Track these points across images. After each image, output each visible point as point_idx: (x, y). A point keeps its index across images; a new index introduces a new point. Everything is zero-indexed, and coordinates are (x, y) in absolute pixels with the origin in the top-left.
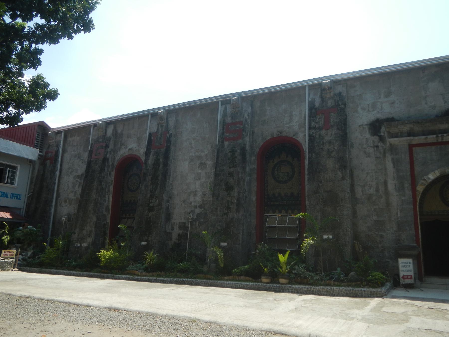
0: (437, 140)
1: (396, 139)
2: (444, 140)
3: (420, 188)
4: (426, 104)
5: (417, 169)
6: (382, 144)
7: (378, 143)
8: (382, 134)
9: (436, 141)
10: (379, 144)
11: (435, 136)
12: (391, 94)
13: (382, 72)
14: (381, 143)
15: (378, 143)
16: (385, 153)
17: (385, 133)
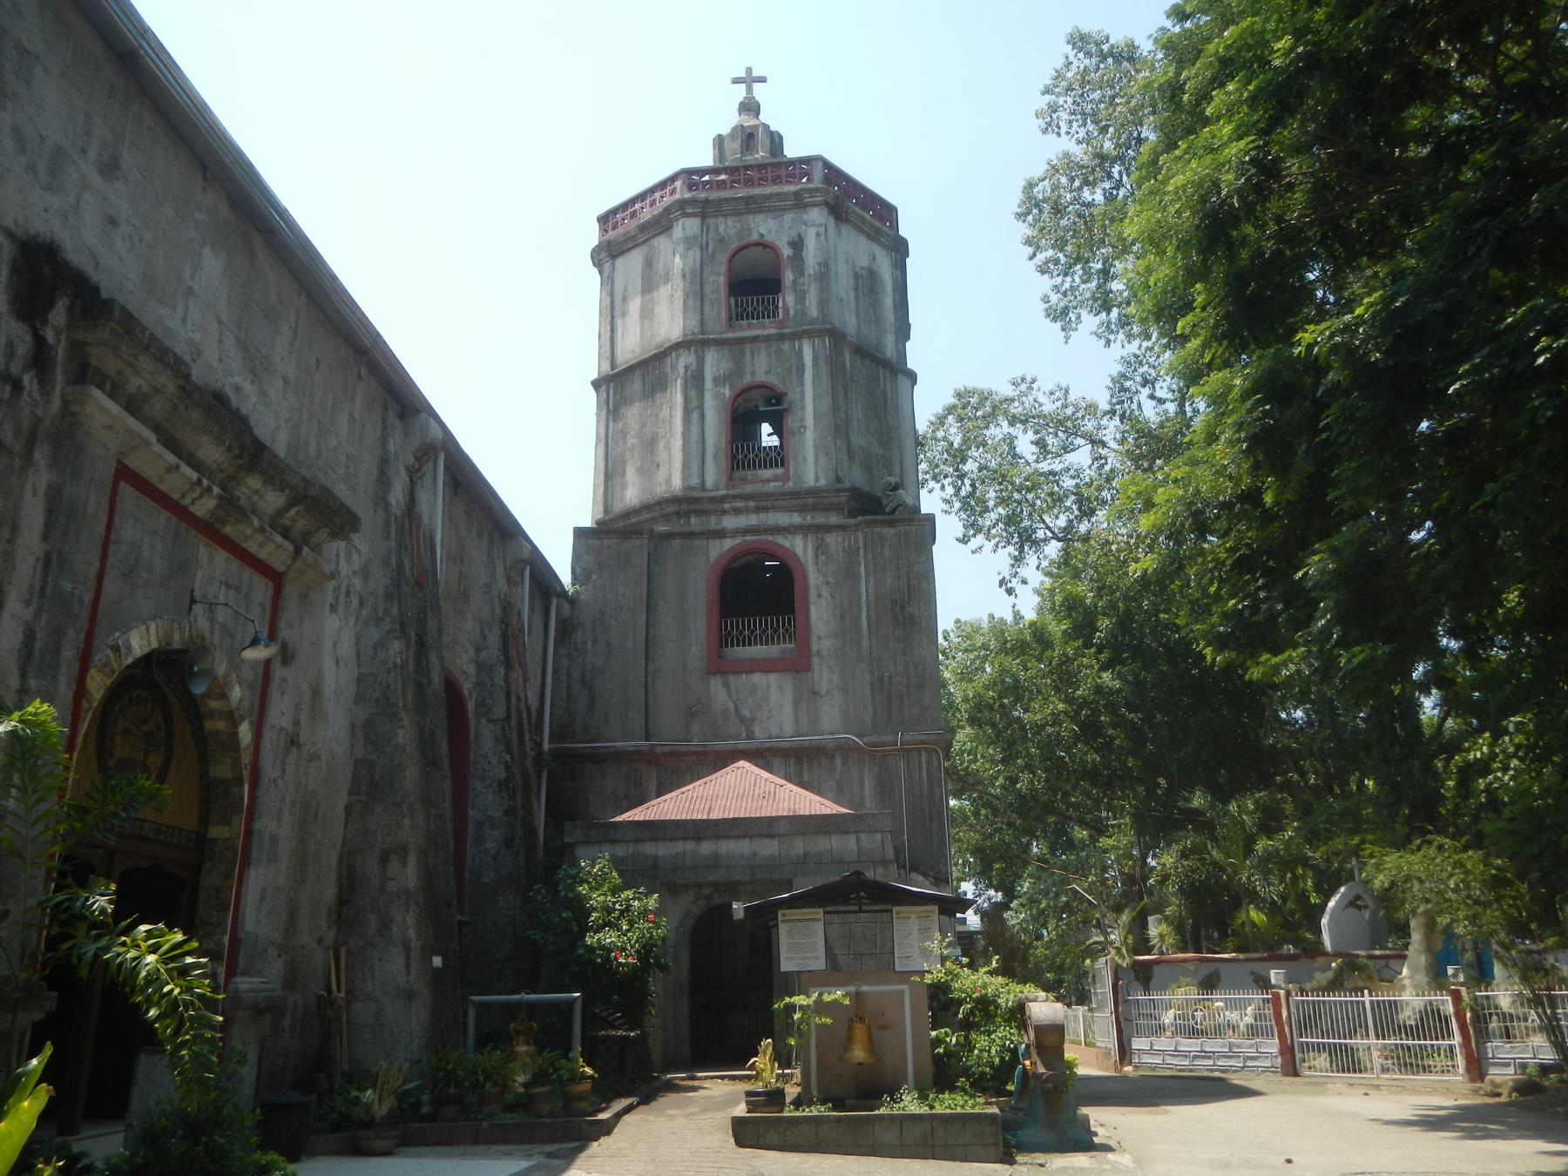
0: (183, 496)
1: (113, 407)
2: (192, 509)
3: (98, 684)
4: (184, 320)
5: (111, 588)
6: (35, 387)
7: (24, 370)
8: (50, 335)
9: (176, 496)
10: (26, 379)
11: (195, 476)
12: (118, 178)
13: (142, 52)
14: (35, 381)
15: (24, 370)
16: (31, 442)
17: (59, 341)
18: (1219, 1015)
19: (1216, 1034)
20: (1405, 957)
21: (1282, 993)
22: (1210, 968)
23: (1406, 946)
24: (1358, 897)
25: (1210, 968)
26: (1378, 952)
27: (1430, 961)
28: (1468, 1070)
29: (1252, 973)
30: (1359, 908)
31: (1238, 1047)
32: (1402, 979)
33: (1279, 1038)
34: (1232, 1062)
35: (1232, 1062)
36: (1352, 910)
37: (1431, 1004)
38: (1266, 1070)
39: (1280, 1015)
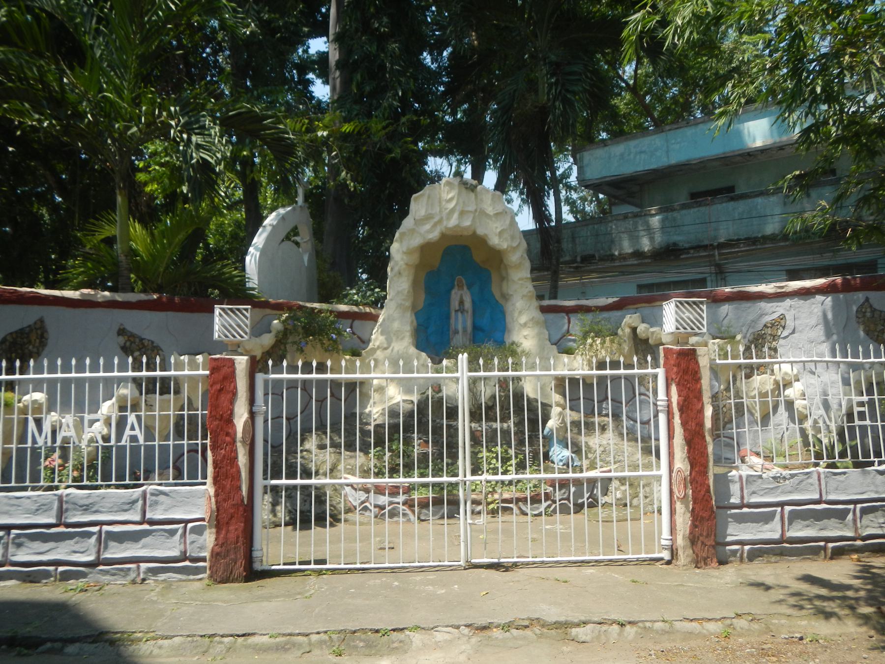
18: (39, 422)
19: (21, 478)
20: (374, 318)
21: (241, 362)
22: (25, 316)
23: (380, 302)
24: (295, 231)
25: (25, 316)
26: (343, 308)
27: (415, 323)
28: (693, 540)
29: (121, 332)
30: (297, 244)
31: (86, 508)
32: (374, 350)
33: (216, 481)
34: (61, 551)
35: (61, 551)
36: (289, 243)
37: (438, 389)
38: (165, 564)
39: (228, 420)
